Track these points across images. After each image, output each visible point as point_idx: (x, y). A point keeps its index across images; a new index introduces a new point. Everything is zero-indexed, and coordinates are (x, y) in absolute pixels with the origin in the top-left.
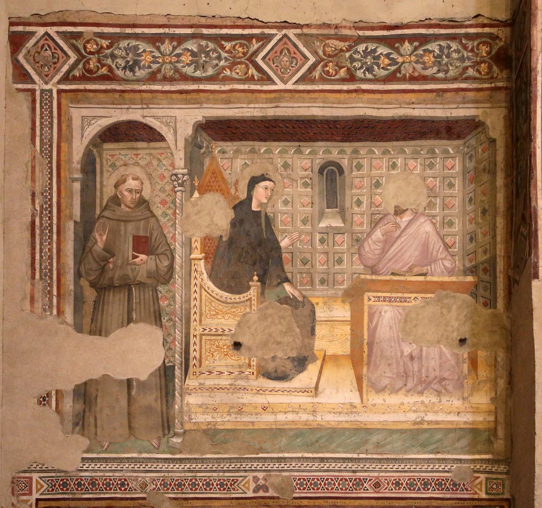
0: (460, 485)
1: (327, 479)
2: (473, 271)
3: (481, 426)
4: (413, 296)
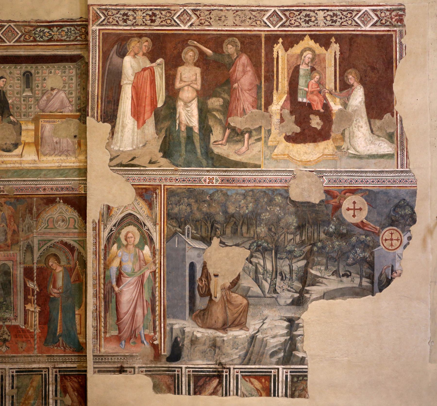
2: (79, 111)
3: (82, 167)
4: (57, 120)
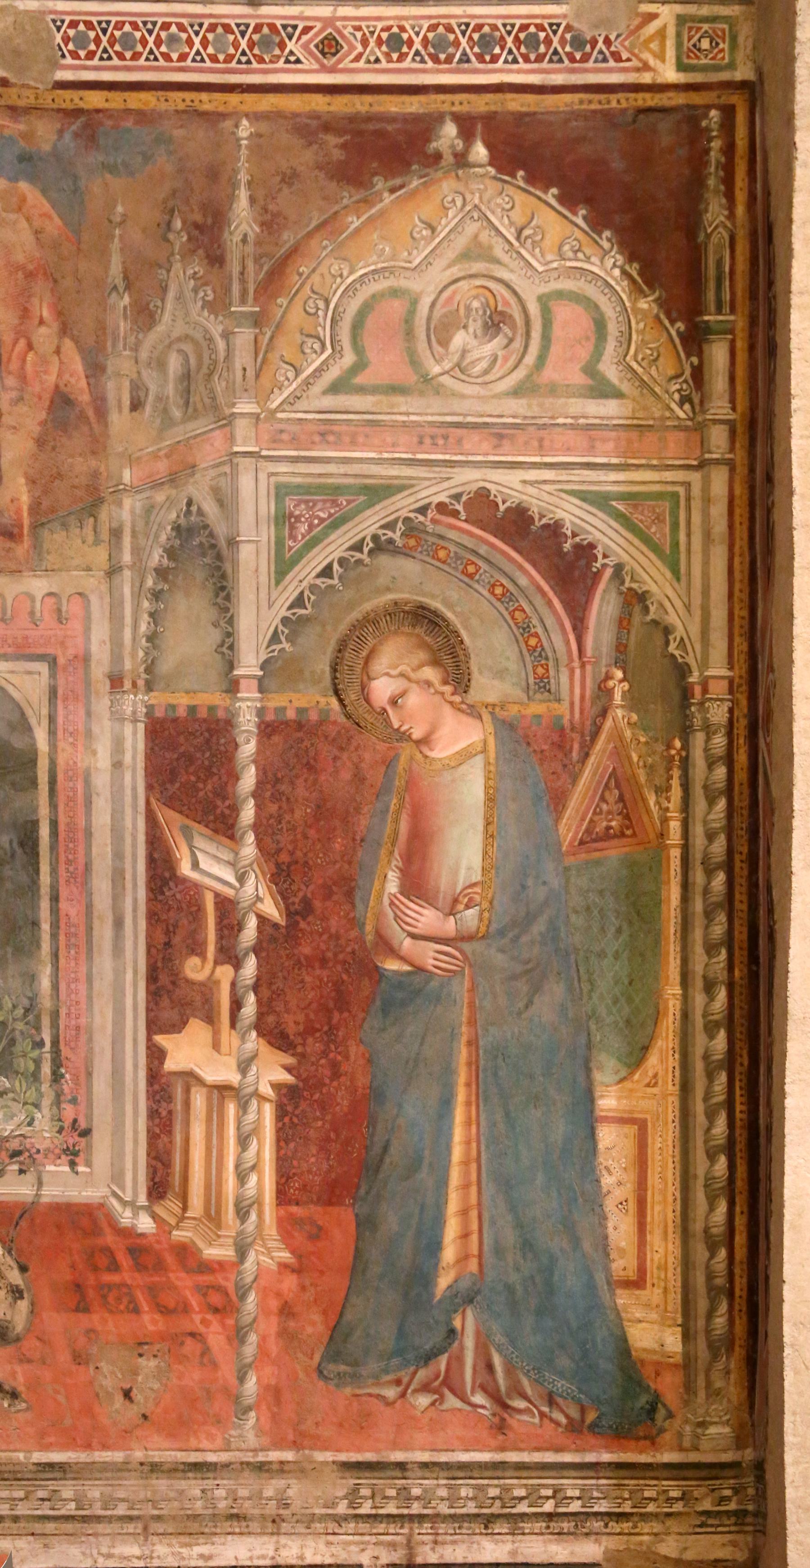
0: (594, 42)
1: (166, 26)
